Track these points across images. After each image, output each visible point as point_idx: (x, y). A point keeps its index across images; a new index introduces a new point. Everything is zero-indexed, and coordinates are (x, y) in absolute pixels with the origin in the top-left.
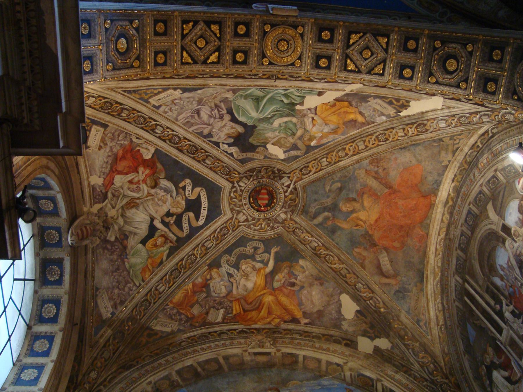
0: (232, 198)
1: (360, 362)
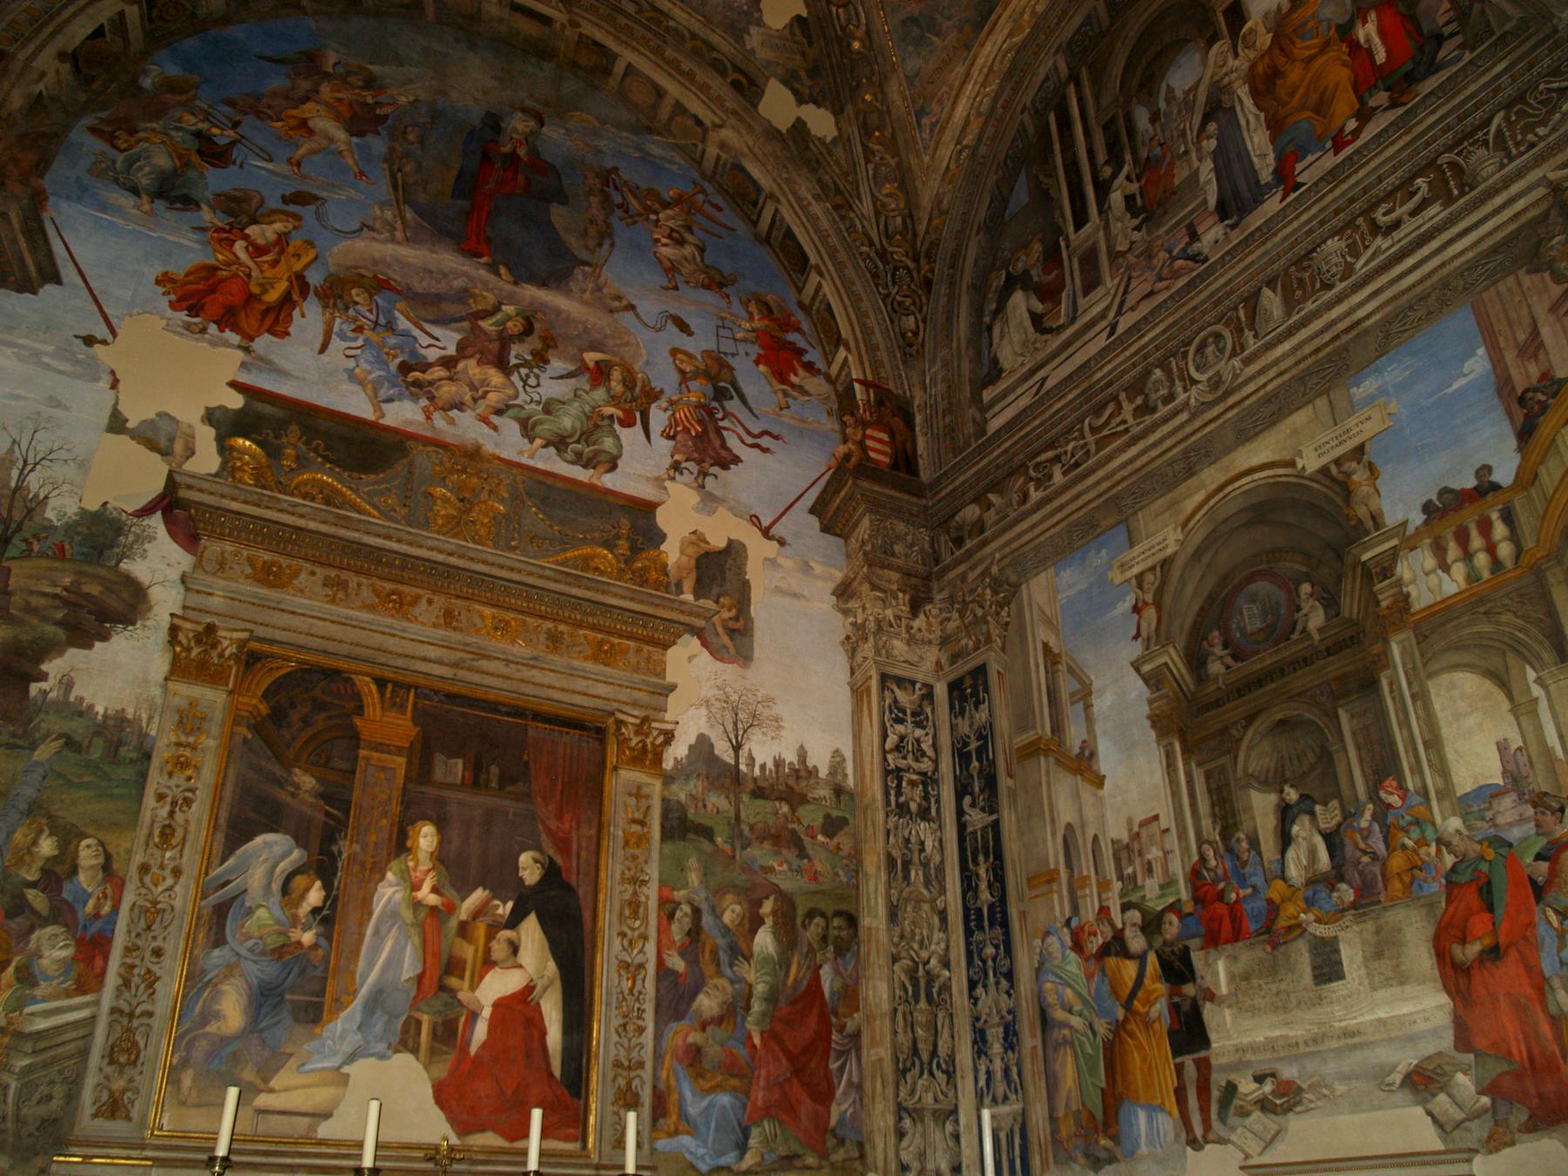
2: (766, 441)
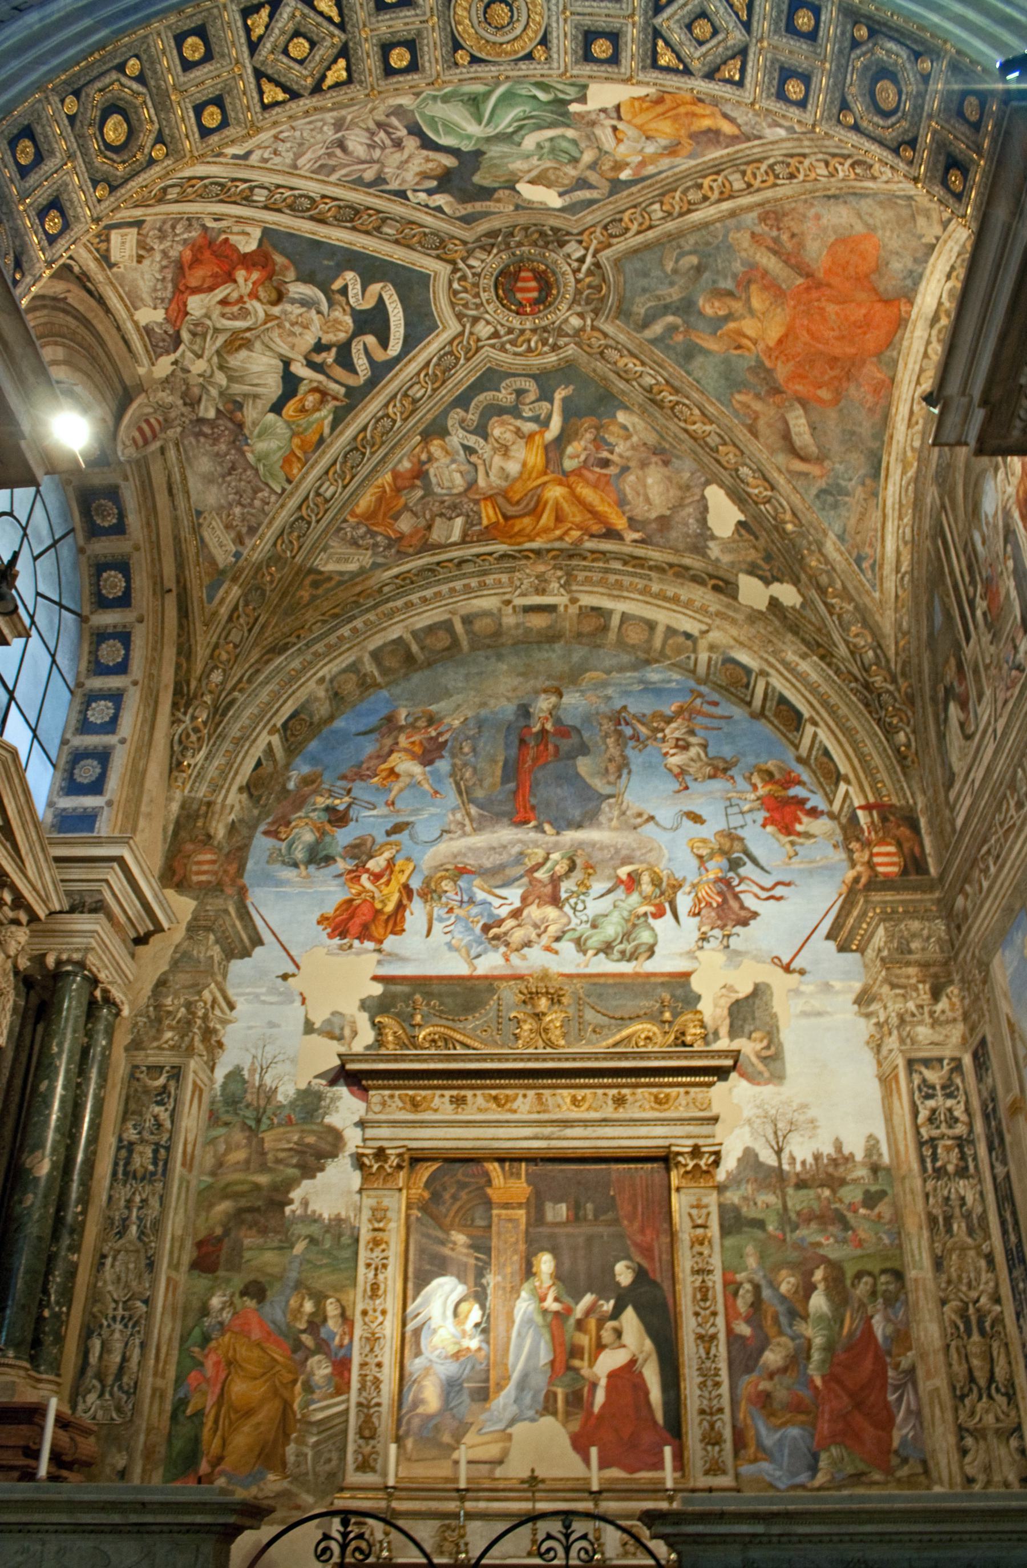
0: (456, 293)
1: (734, 632)
2: (779, 891)
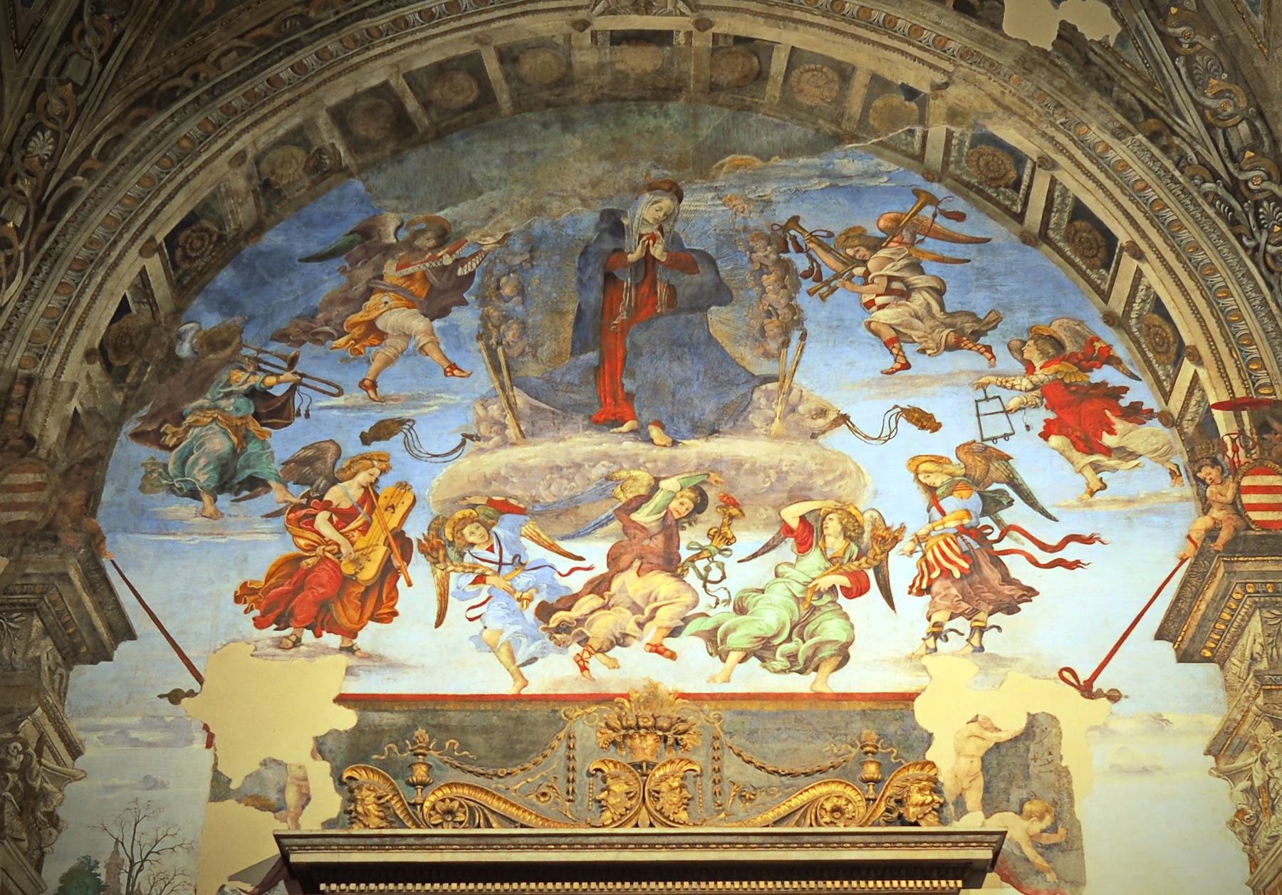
1: (994, 88)
